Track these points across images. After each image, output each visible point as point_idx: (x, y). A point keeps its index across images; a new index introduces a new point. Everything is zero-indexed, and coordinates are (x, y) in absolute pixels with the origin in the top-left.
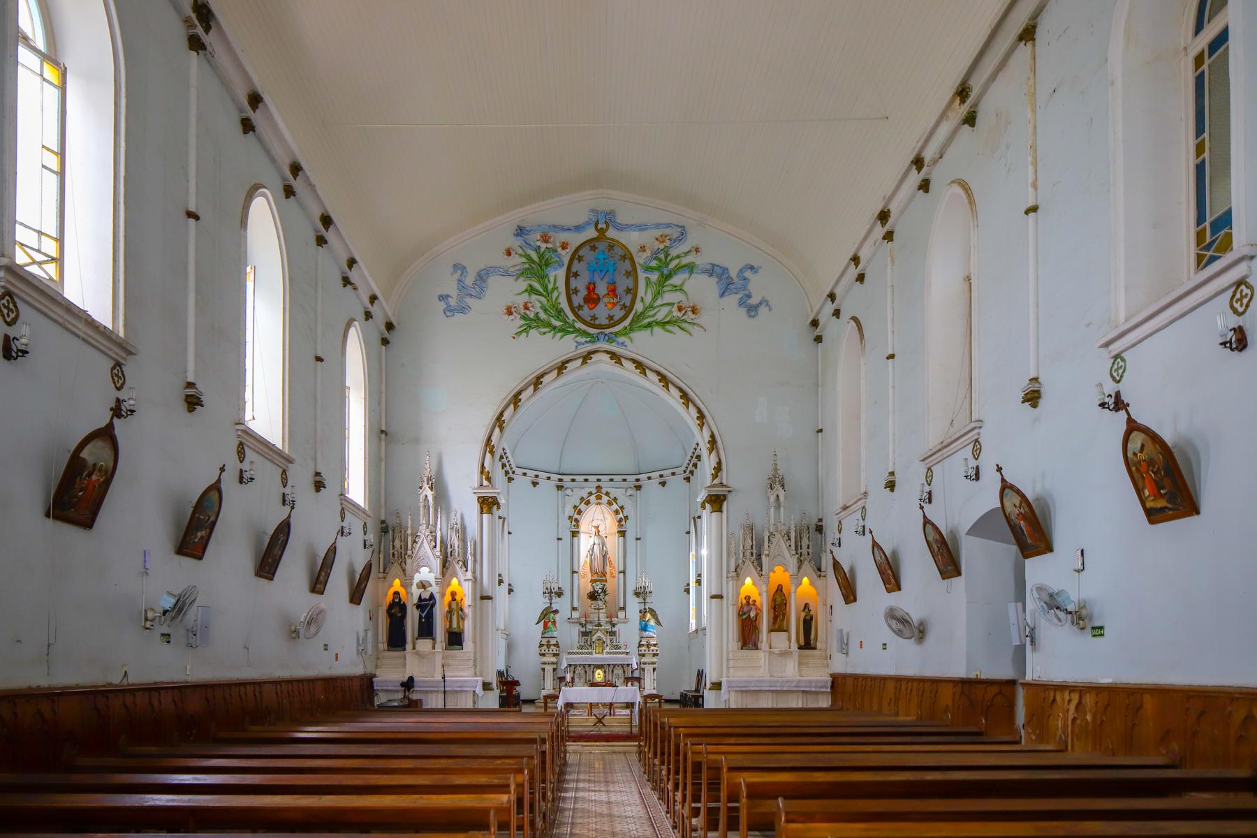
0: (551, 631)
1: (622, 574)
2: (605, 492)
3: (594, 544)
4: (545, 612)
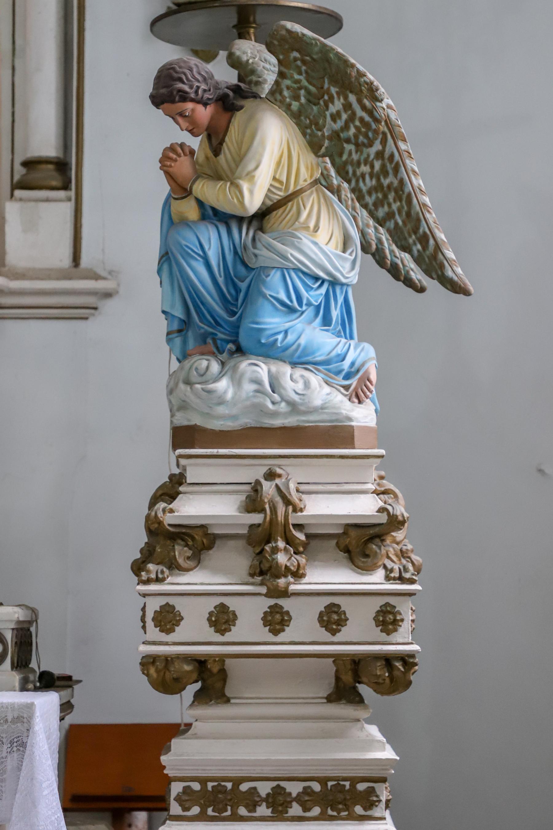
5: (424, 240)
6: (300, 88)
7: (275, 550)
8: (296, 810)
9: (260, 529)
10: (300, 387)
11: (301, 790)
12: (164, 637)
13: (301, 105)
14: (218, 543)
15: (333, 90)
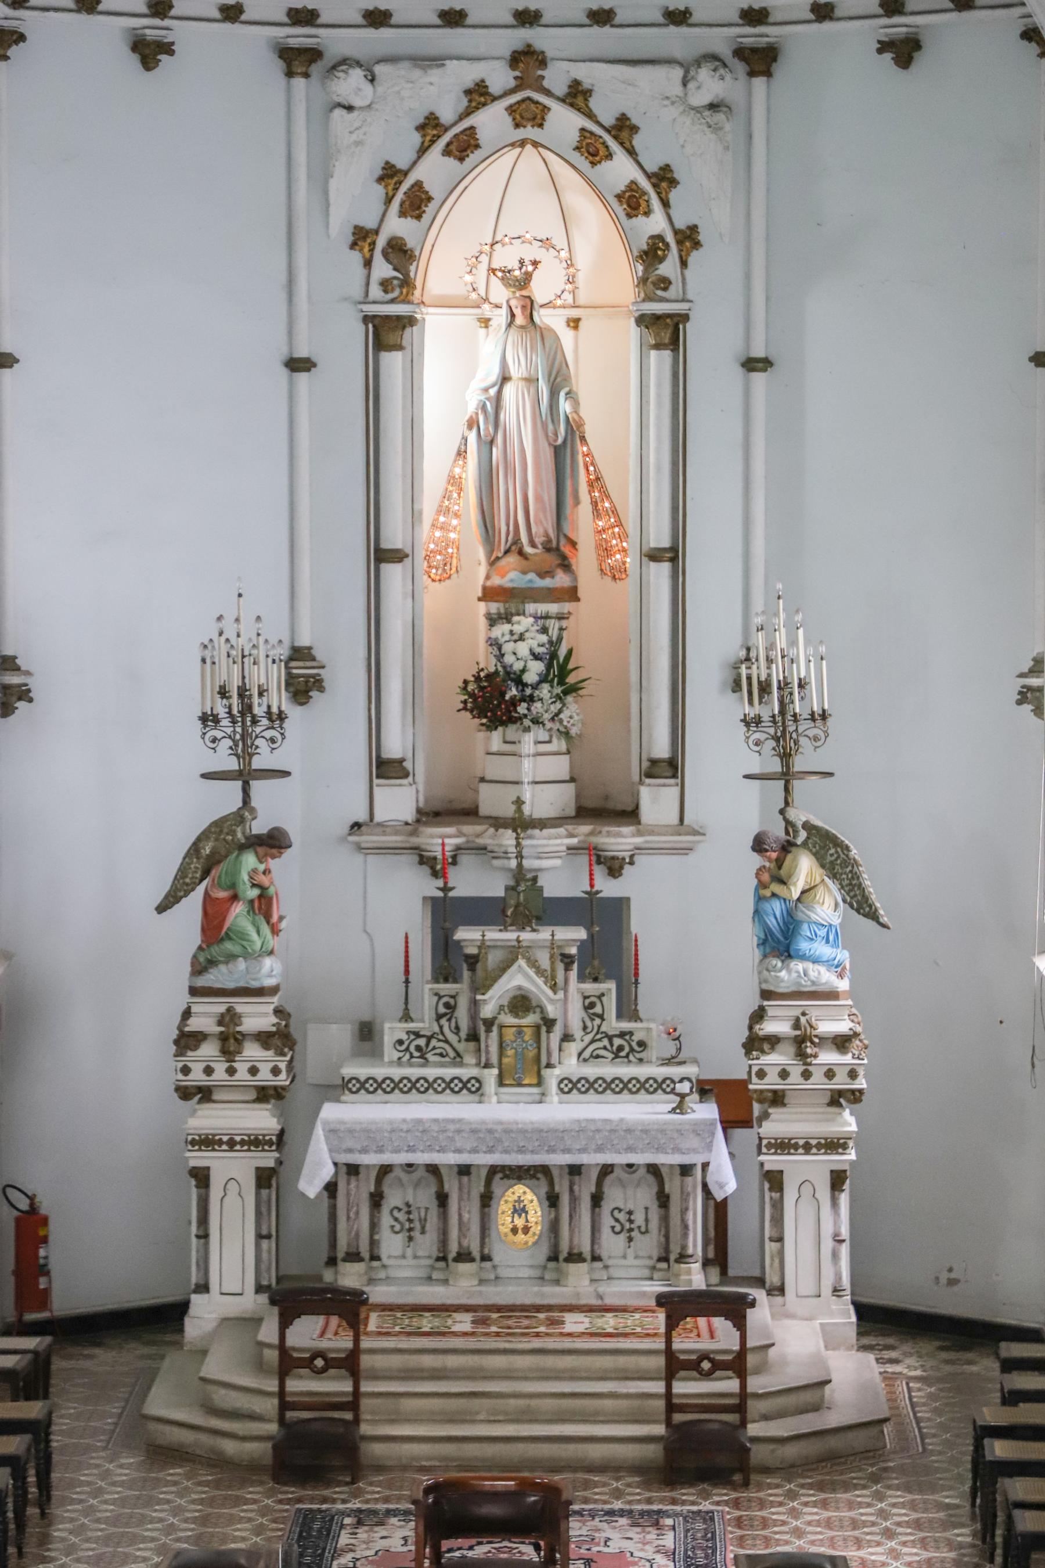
0: (246, 955)
1: (665, 567)
2: (560, 88)
3: (505, 379)
5: (870, 906)
7: (806, 1047)
8: (814, 1150)
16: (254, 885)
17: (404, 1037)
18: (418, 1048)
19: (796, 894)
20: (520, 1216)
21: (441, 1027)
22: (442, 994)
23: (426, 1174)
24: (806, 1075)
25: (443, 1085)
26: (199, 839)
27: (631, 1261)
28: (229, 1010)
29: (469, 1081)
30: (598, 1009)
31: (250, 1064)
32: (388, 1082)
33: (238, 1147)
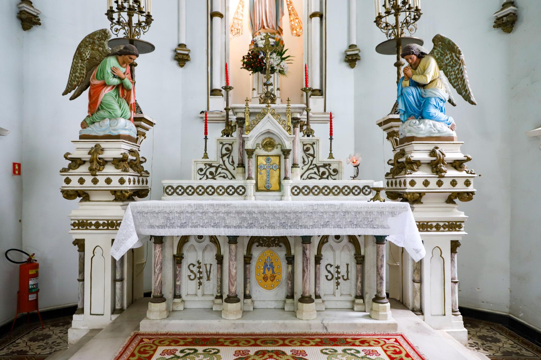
4: (87, 55)
5: (466, 91)
6: (439, 52)
7: (441, 166)
8: (442, 229)
9: (436, 161)
10: (440, 127)
11: (443, 224)
12: (411, 188)
13: (439, 56)
14: (422, 165)
15: (448, 52)
16: (114, 76)
17: (203, 167)
18: (211, 173)
19: (429, 81)
20: (269, 269)
21: (224, 162)
22: (224, 143)
23: (210, 243)
24: (440, 184)
25: (223, 190)
26: (80, 47)
27: (338, 297)
28: (96, 146)
29: (238, 188)
30: (311, 152)
31: (106, 177)
32: (190, 188)
33: (101, 227)
